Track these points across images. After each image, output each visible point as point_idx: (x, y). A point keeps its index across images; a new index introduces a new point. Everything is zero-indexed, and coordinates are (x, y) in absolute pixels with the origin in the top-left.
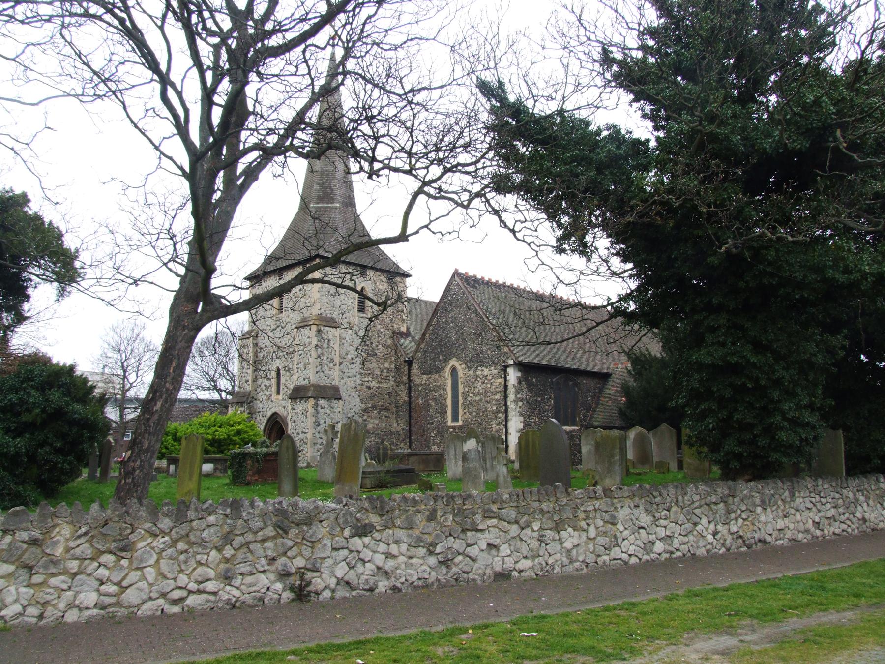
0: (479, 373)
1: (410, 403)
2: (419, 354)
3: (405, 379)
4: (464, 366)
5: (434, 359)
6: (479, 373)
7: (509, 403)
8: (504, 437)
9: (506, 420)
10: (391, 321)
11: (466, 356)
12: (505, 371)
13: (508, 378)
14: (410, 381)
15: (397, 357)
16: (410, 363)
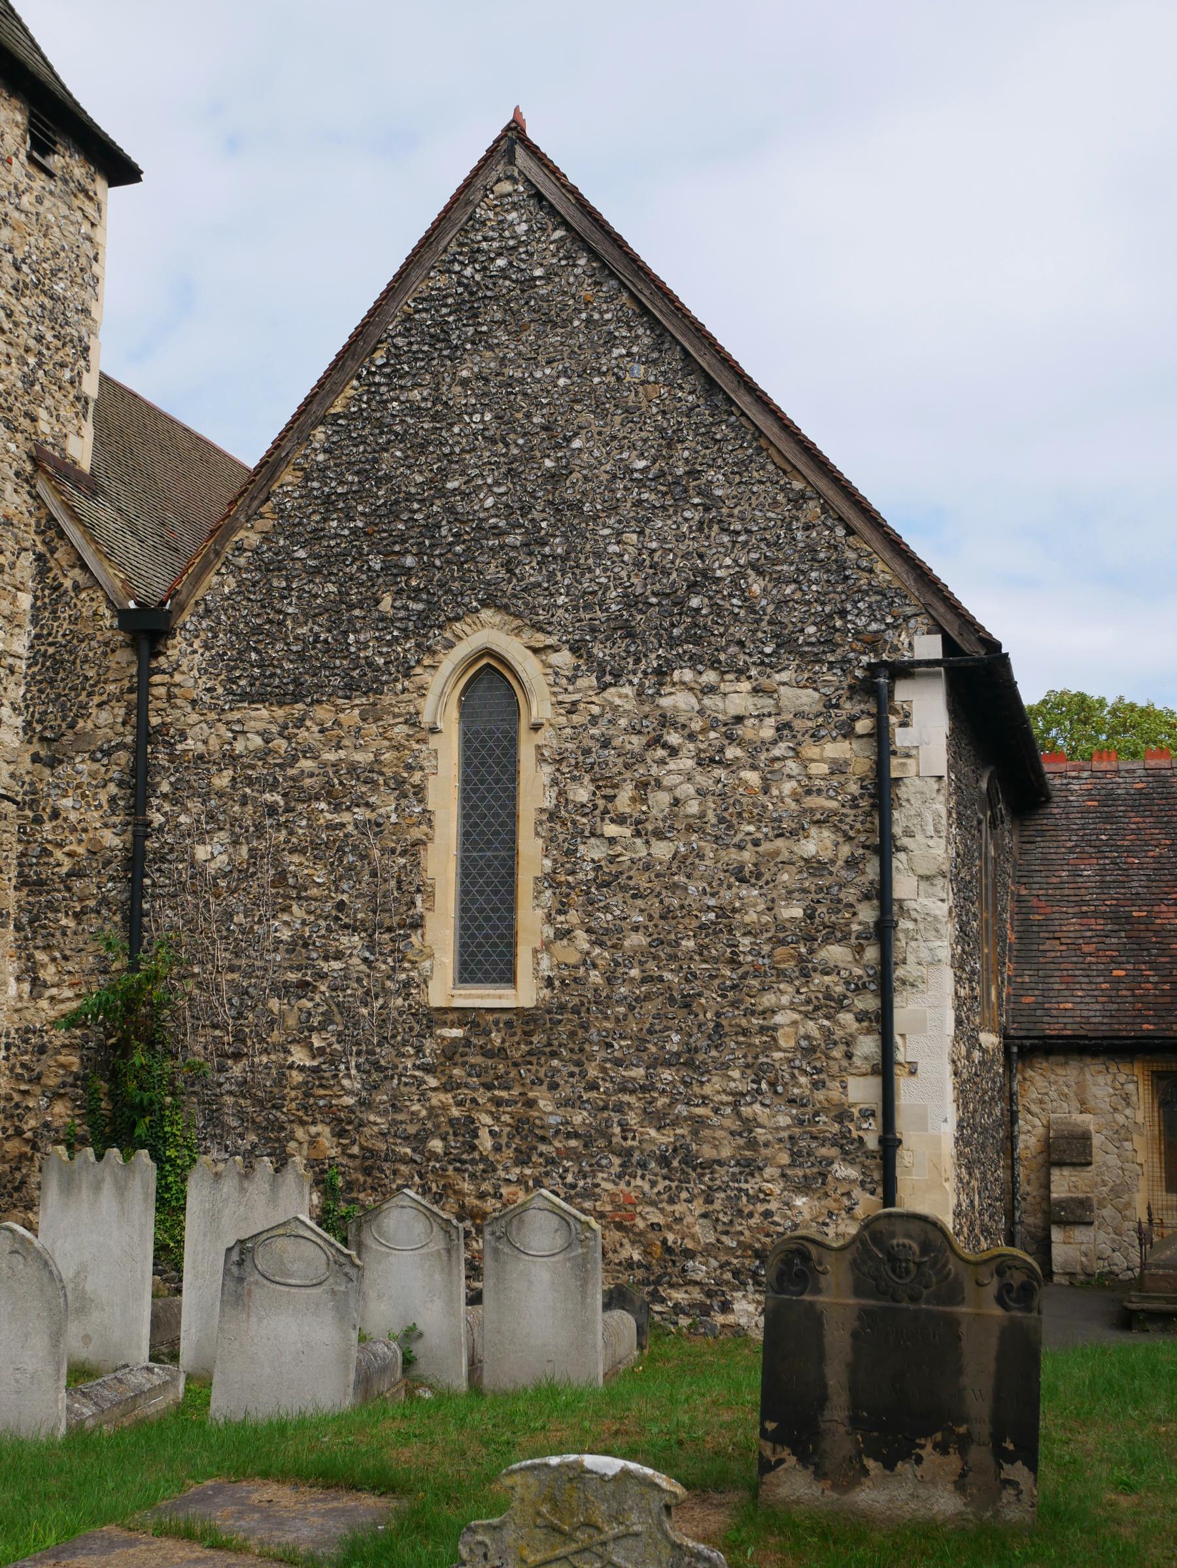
0: (679, 701)
1: (135, 862)
2: (219, 584)
3: (105, 720)
4: (564, 659)
5: (336, 612)
6: (679, 701)
7: (903, 886)
8: (862, 1091)
9: (884, 982)
10: (29, 381)
11: (584, 602)
12: (883, 709)
13: (901, 738)
14: (145, 735)
15: (50, 597)
16: (147, 630)
